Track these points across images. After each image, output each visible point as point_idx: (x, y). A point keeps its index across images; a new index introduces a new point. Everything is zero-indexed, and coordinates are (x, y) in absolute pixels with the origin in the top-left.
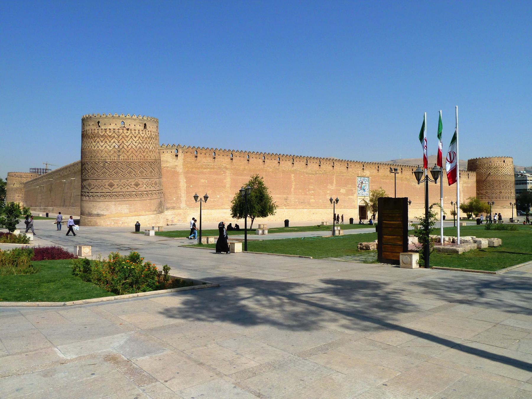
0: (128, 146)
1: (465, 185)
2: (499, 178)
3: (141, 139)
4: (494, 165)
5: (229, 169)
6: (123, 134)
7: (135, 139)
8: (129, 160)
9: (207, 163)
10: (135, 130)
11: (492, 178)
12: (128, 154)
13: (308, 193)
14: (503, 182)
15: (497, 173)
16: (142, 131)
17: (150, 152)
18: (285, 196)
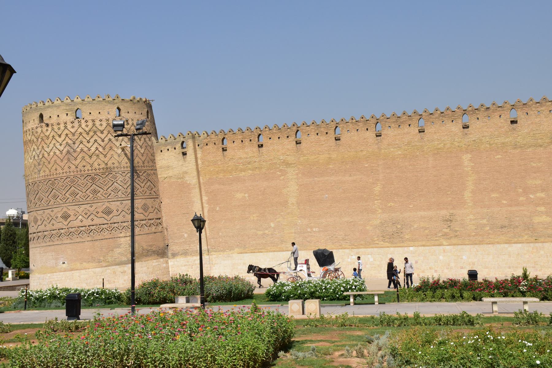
0: (50, 154)
3: (70, 138)
5: (294, 164)
6: (42, 135)
7: (60, 140)
8: (52, 177)
9: (247, 158)
10: (59, 124)
12: (50, 166)
13: (521, 199)
16: (72, 122)
17: (91, 157)
18: (444, 212)
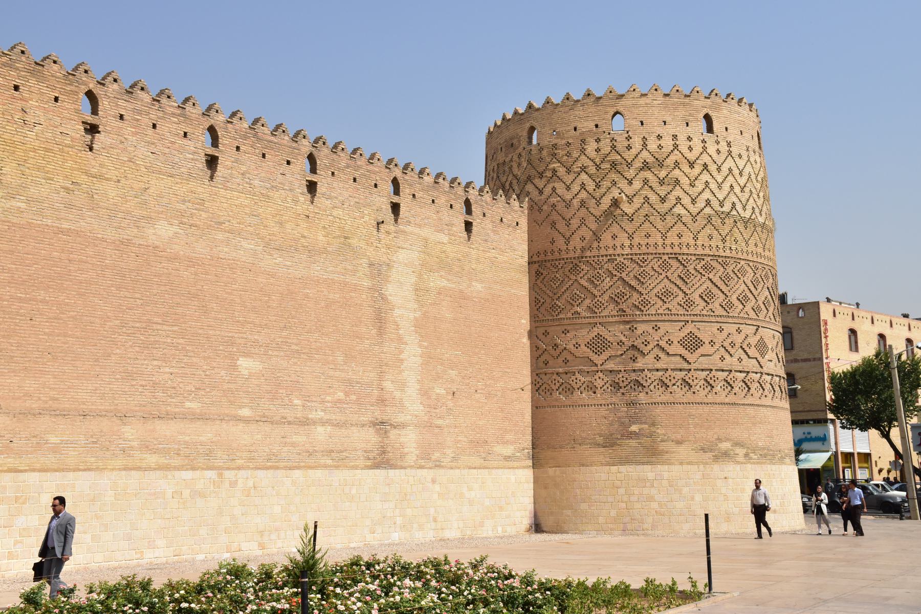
1: (437, 281)
2: (676, 241)
4: (645, 145)
11: (631, 237)
14: (708, 268)
15: (667, 205)
